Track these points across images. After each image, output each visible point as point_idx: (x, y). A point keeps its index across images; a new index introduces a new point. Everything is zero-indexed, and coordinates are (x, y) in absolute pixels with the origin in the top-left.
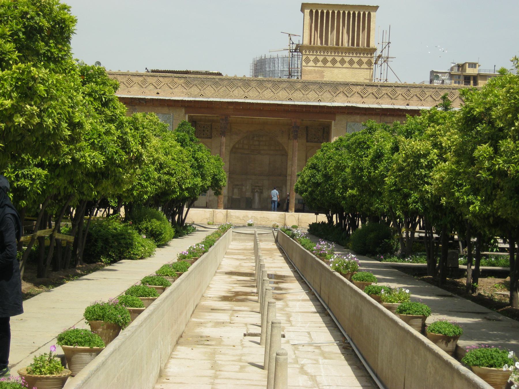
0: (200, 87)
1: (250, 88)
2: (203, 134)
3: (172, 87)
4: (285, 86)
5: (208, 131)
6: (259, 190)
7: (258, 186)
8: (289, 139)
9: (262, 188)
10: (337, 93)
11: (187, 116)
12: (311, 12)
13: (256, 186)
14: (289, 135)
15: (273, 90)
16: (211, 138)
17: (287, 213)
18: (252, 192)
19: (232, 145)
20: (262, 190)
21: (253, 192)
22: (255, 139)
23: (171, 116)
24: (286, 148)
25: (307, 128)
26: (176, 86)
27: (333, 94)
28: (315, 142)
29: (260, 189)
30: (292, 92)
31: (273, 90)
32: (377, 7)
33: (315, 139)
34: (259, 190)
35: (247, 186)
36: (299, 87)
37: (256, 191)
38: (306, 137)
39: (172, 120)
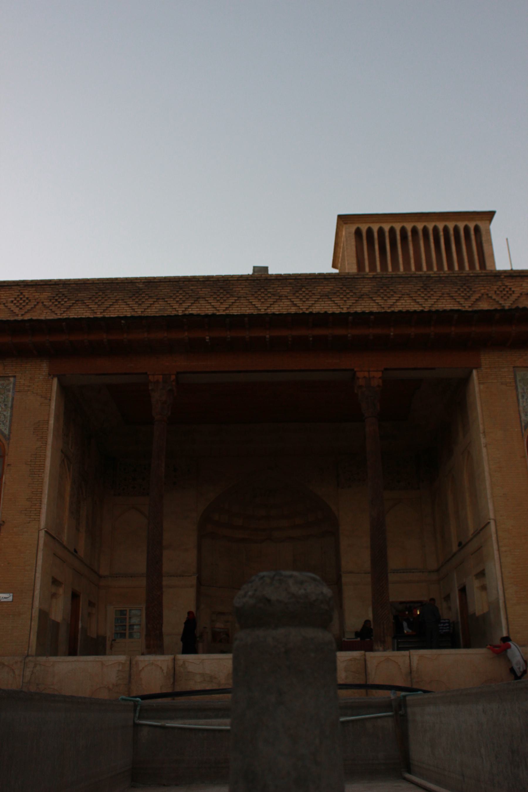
0: (93, 306)
1: (232, 300)
3: (17, 310)
4: (327, 289)
10: (473, 299)
11: (55, 381)
12: (358, 232)
15: (297, 301)
17: (369, 654)
23: (8, 384)
26: (28, 307)
27: (462, 301)
30: (349, 303)
31: (297, 301)
32: (490, 215)
36: (365, 290)
39: (10, 394)
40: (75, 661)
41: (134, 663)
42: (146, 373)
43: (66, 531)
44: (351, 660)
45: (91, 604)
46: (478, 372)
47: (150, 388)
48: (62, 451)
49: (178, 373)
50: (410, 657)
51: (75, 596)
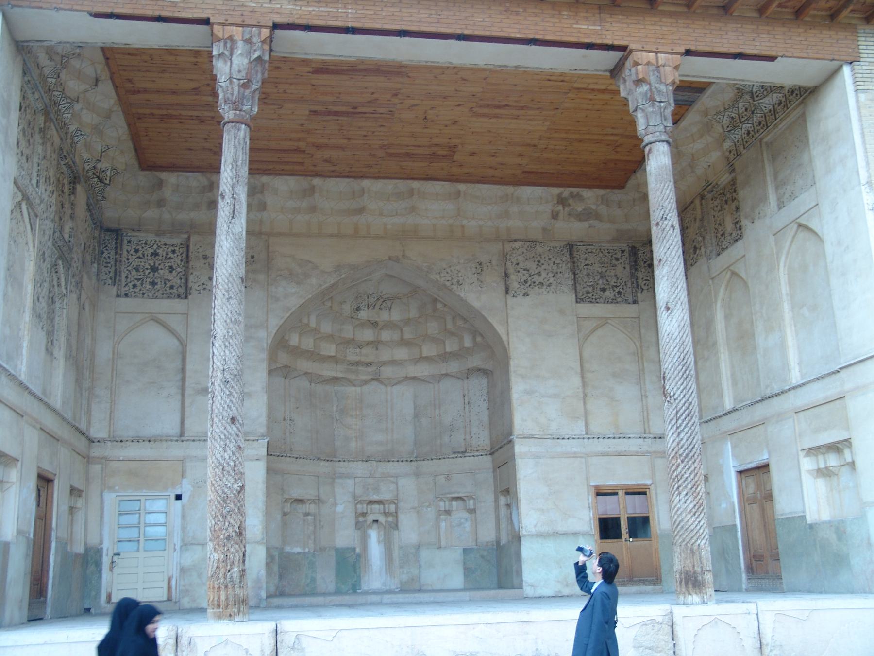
2: (153, 284)
5: (171, 269)
6: (382, 519)
7: (379, 502)
8: (507, 291)
9: (392, 508)
13: (372, 502)
14: (507, 275)
16: (186, 298)
18: (357, 523)
19: (274, 323)
20: (396, 515)
21: (361, 524)
22: (363, 314)
24: (501, 330)
25: (571, 247)
28: (607, 302)
29: (386, 514)
33: (604, 290)
34: (382, 519)
35: (335, 504)
37: (370, 518)
38: (571, 283)
40: (45, 644)
41: (184, 641)
42: (206, 22)
43: (25, 352)
44: (644, 624)
45: (75, 492)
46: (853, 70)
47: (215, 53)
48: (15, 182)
49: (276, 26)
50: (757, 614)
51: (45, 481)
